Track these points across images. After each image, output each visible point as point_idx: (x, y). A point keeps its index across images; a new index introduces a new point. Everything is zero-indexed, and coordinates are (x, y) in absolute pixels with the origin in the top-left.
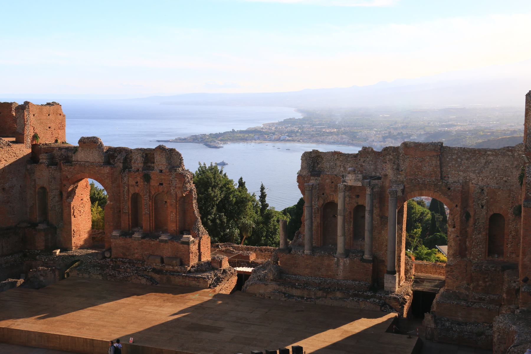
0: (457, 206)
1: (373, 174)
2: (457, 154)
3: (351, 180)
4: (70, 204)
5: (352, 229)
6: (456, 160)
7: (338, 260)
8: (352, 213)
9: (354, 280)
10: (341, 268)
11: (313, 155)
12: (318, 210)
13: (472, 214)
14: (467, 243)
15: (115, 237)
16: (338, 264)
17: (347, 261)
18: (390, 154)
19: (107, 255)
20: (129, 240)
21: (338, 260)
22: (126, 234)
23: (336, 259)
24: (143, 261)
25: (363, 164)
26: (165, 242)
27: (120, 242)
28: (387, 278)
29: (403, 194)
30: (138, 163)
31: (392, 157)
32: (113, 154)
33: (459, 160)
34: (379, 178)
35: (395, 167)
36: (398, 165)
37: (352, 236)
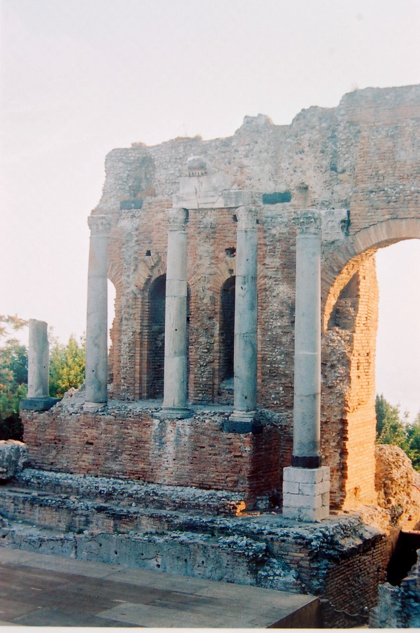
5: (216, 347)
8: (218, 298)
9: (202, 486)
10: (170, 449)
11: (133, 156)
12: (135, 298)
18: (313, 128)
21: (162, 428)
23: (156, 422)
25: (246, 162)
28: (292, 476)
29: (347, 234)
31: (316, 136)
34: (285, 197)
36: (335, 154)
37: (216, 366)
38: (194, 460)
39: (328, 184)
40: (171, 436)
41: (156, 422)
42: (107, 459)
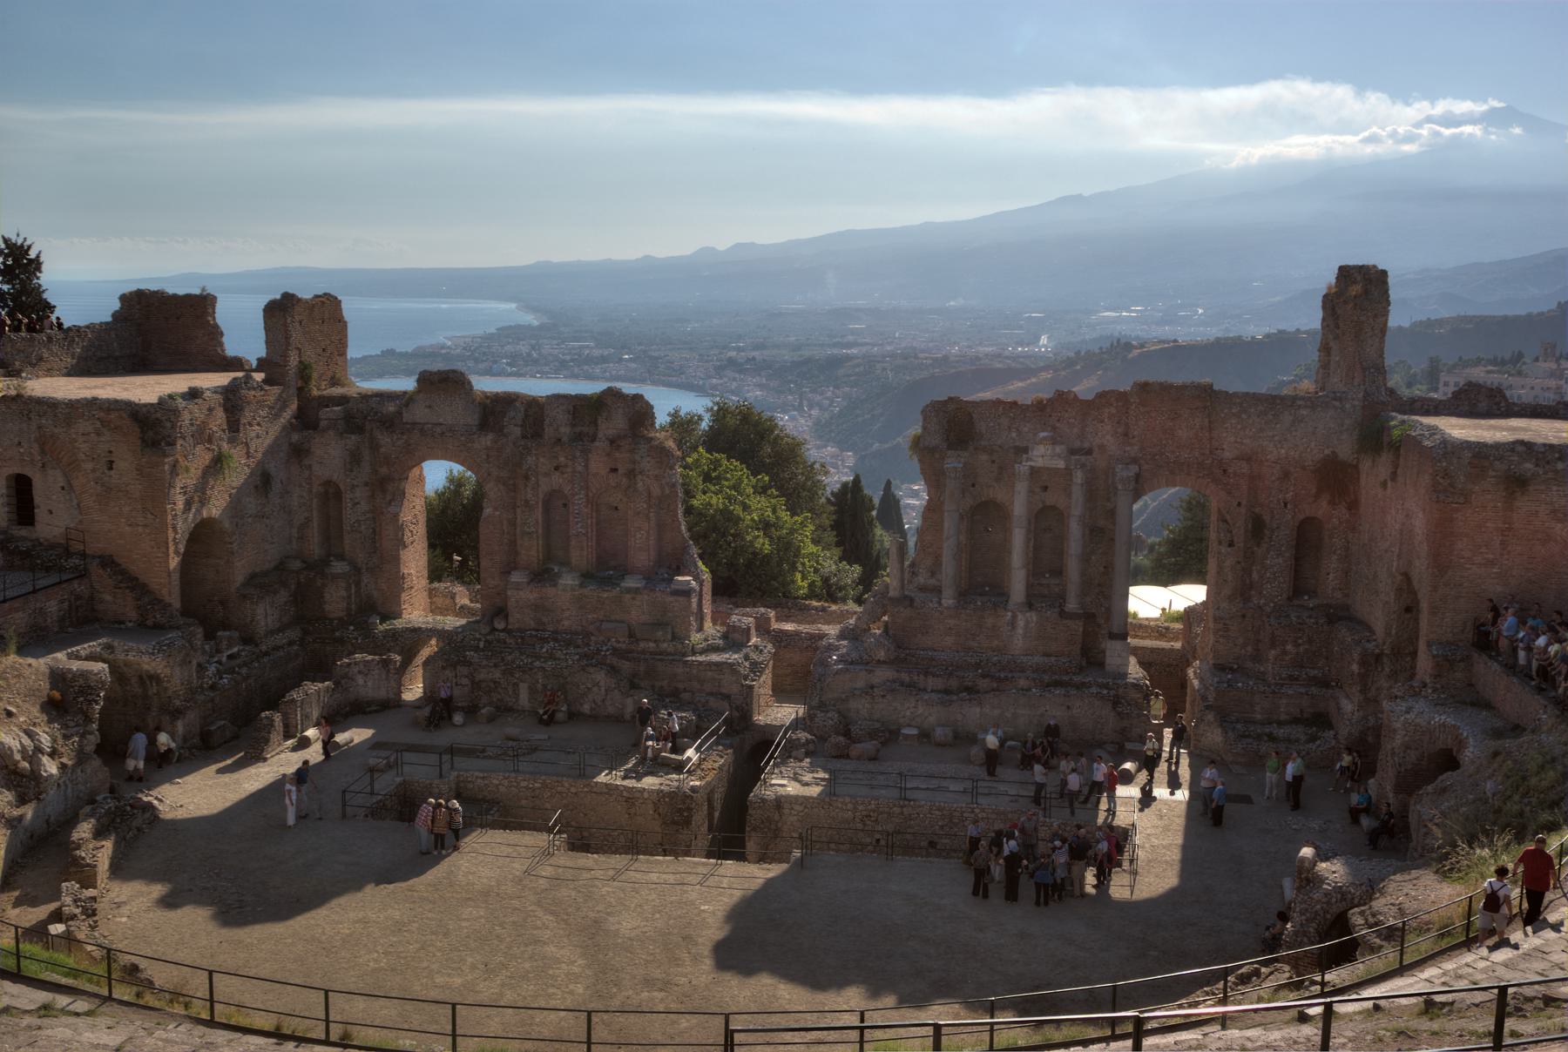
1: (1077, 444)
3: (1043, 456)
4: (396, 516)
9: (1046, 655)
13: (1267, 518)
14: (1255, 576)
15: (518, 587)
16: (1013, 624)
17: (1033, 616)
19: (500, 625)
20: (550, 591)
21: (1014, 617)
22: (542, 575)
24: (588, 635)
26: (637, 591)
27: (530, 595)
31: (1113, 411)
32: (496, 409)
34: (1089, 452)
40: (1021, 623)
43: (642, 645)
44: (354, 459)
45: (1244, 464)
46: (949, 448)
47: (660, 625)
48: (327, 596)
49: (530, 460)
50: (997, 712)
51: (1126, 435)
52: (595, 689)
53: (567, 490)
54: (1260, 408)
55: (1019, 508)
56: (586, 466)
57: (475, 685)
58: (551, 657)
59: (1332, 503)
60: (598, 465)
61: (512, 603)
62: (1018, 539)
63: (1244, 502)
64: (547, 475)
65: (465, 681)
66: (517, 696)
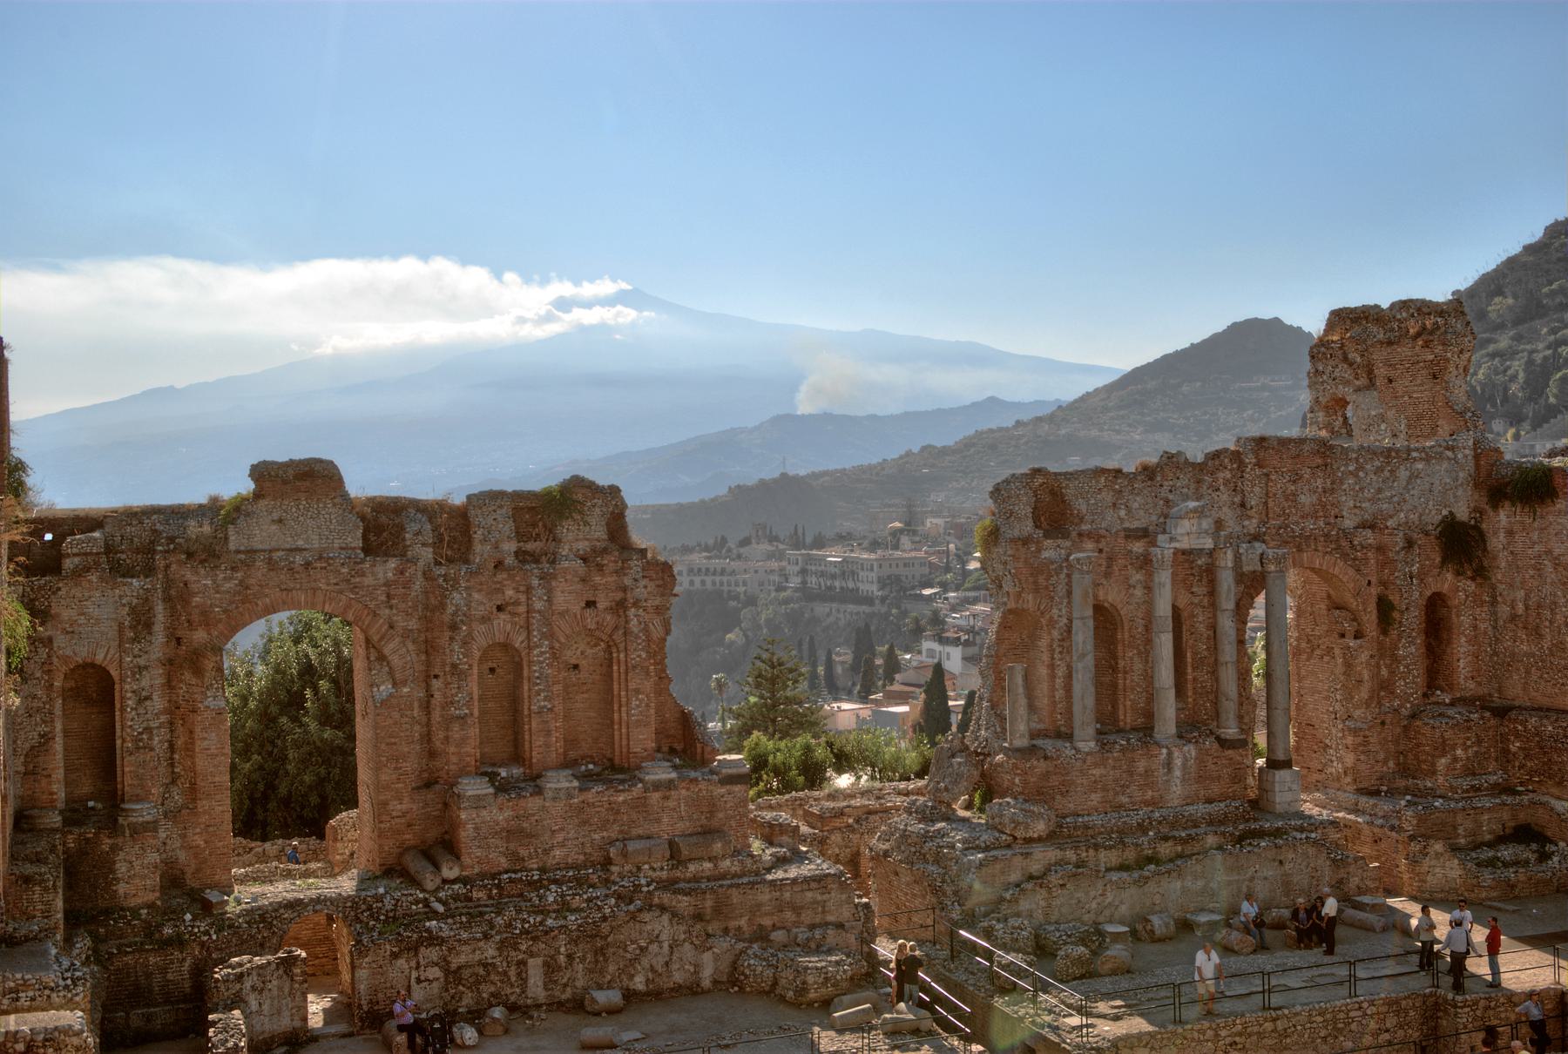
0: (1369, 583)
2: (1357, 459)
6: (1354, 474)
7: (1170, 754)
9: (1209, 801)
10: (1178, 773)
15: (478, 803)
16: (1169, 764)
17: (1191, 750)
20: (533, 804)
21: (1170, 754)
23: (1164, 751)
26: (670, 785)
27: (499, 814)
30: (496, 539)
33: (1361, 474)
35: (1237, 499)
38: (1200, 779)
39: (1242, 517)
40: (1178, 762)
41: (1164, 751)
42: (1117, 794)
43: (692, 868)
44: (141, 621)
45: (1369, 533)
46: (1046, 536)
47: (708, 833)
48: (122, 868)
49: (457, 597)
50: (1200, 883)
51: (1243, 505)
52: (654, 948)
53: (518, 641)
54: (1377, 463)
55: (1163, 608)
56: (549, 601)
57: (453, 975)
58: (564, 908)
59: (1458, 574)
60: (566, 596)
61: (466, 834)
62: (1165, 644)
63: (1374, 580)
64: (485, 620)
65: (435, 972)
66: (523, 980)
